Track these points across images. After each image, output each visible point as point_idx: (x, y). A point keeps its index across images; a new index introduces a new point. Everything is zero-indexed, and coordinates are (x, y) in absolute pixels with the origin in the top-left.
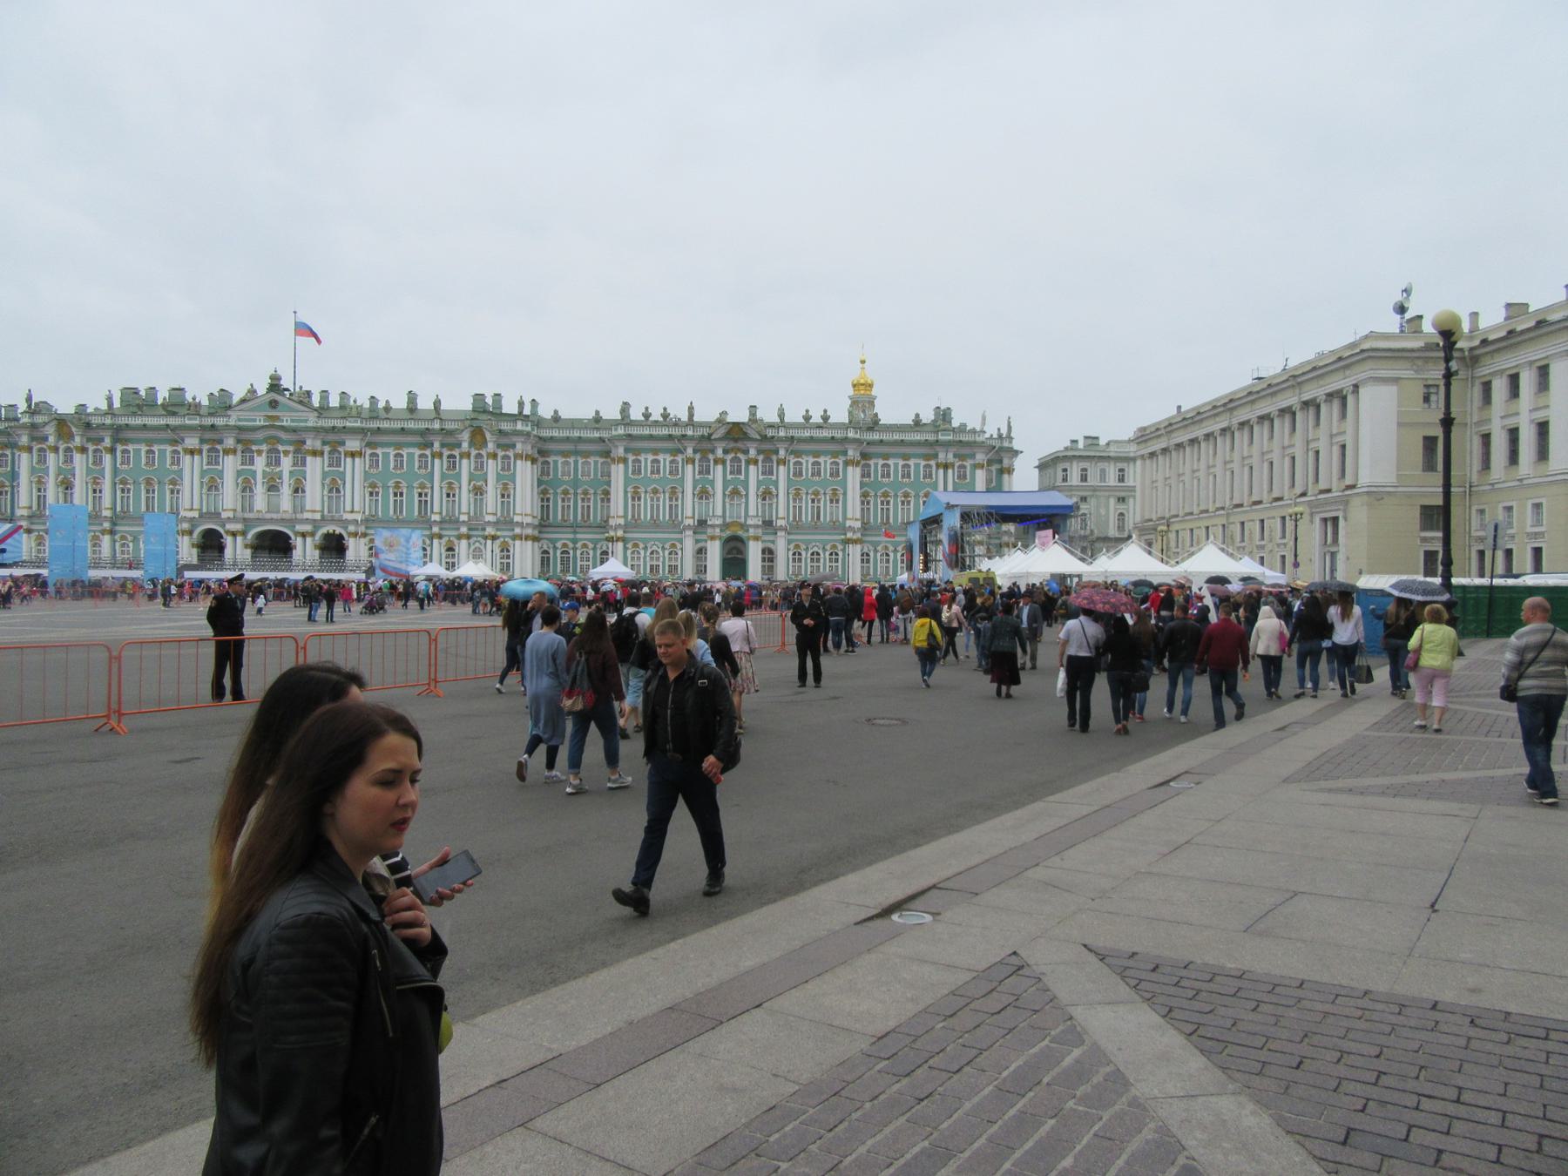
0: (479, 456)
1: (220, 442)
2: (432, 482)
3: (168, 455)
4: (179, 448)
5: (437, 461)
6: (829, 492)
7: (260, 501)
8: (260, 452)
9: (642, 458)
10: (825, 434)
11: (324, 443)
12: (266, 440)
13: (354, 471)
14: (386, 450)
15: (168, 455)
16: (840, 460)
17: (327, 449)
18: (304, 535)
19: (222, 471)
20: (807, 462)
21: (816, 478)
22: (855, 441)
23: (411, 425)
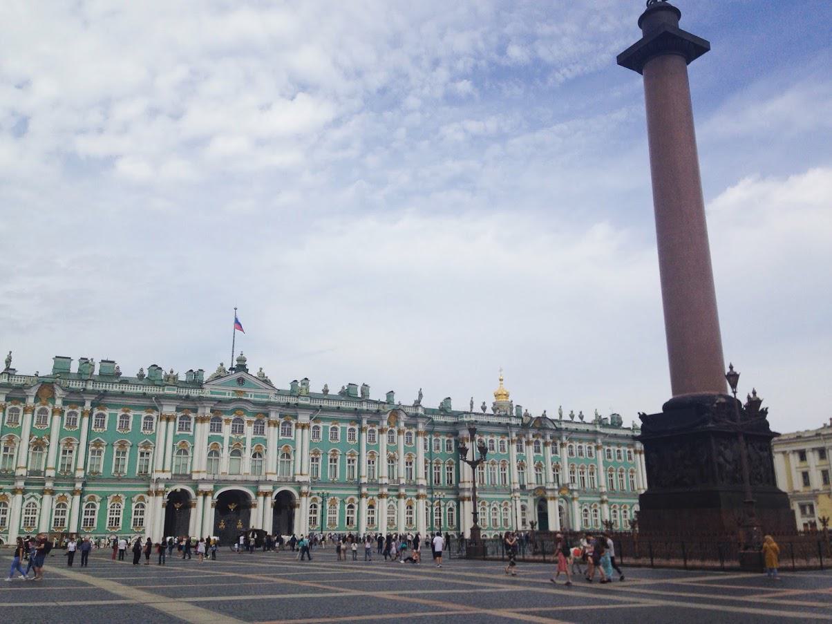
0: (391, 432)
1: (195, 411)
2: (359, 450)
3: (143, 419)
4: (154, 415)
5: (364, 434)
7: (225, 464)
8: (227, 421)
10: (583, 427)
11: (281, 416)
12: (233, 411)
13: (303, 440)
14: (326, 424)
15: (143, 419)
16: (593, 446)
17: (282, 420)
18: (266, 495)
19: (193, 437)
20: (576, 445)
22: (601, 433)
23: (343, 405)
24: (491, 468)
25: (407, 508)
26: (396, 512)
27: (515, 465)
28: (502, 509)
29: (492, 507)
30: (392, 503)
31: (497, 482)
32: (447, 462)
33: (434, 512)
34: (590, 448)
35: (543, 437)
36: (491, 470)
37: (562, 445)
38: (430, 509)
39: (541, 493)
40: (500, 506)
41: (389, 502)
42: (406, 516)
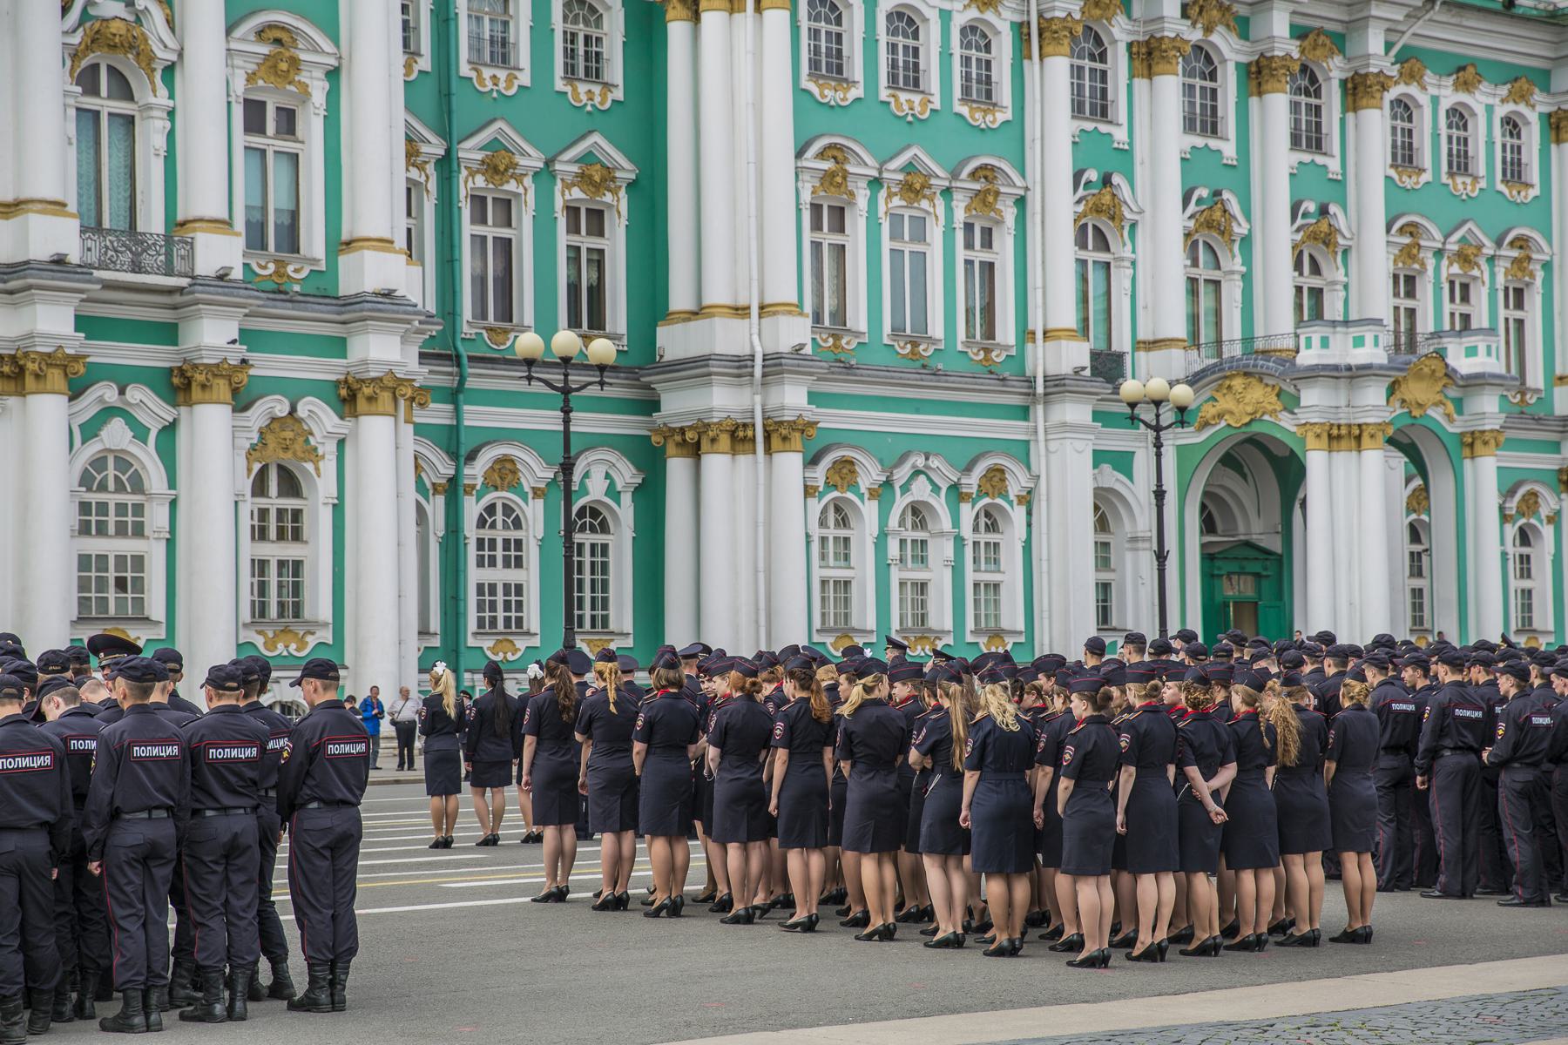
24: (896, 219)
25: (260, 488)
26: (157, 517)
27: (1059, 208)
28: (967, 512)
29: (901, 502)
30: (116, 435)
31: (937, 329)
32: (566, 166)
33: (470, 531)
34: (1512, 125)
35: (1243, 28)
36: (896, 235)
37: (1357, 90)
38: (436, 508)
39: (1246, 404)
40: (957, 494)
41: (90, 430)
42: (249, 550)
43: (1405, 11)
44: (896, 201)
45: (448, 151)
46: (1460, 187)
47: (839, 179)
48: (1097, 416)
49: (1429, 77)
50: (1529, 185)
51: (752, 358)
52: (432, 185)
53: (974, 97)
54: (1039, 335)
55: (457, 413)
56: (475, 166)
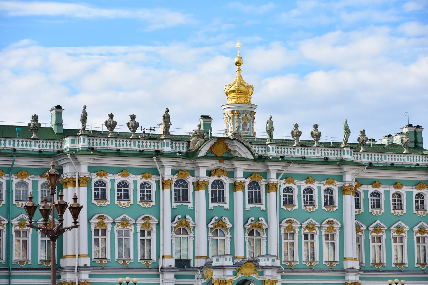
6: (325, 225)
9: (107, 179)
16: (335, 188)
21: (309, 208)
24: (119, 232)
31: (132, 257)
43: (281, 167)
44: (120, 227)
45: (9, 222)
46: (308, 209)
47: (102, 224)
48: (176, 276)
49: (296, 181)
50: (335, 206)
51: (75, 267)
52: (5, 230)
53: (145, 200)
54: (161, 257)
55: (9, 281)
56: (16, 225)
